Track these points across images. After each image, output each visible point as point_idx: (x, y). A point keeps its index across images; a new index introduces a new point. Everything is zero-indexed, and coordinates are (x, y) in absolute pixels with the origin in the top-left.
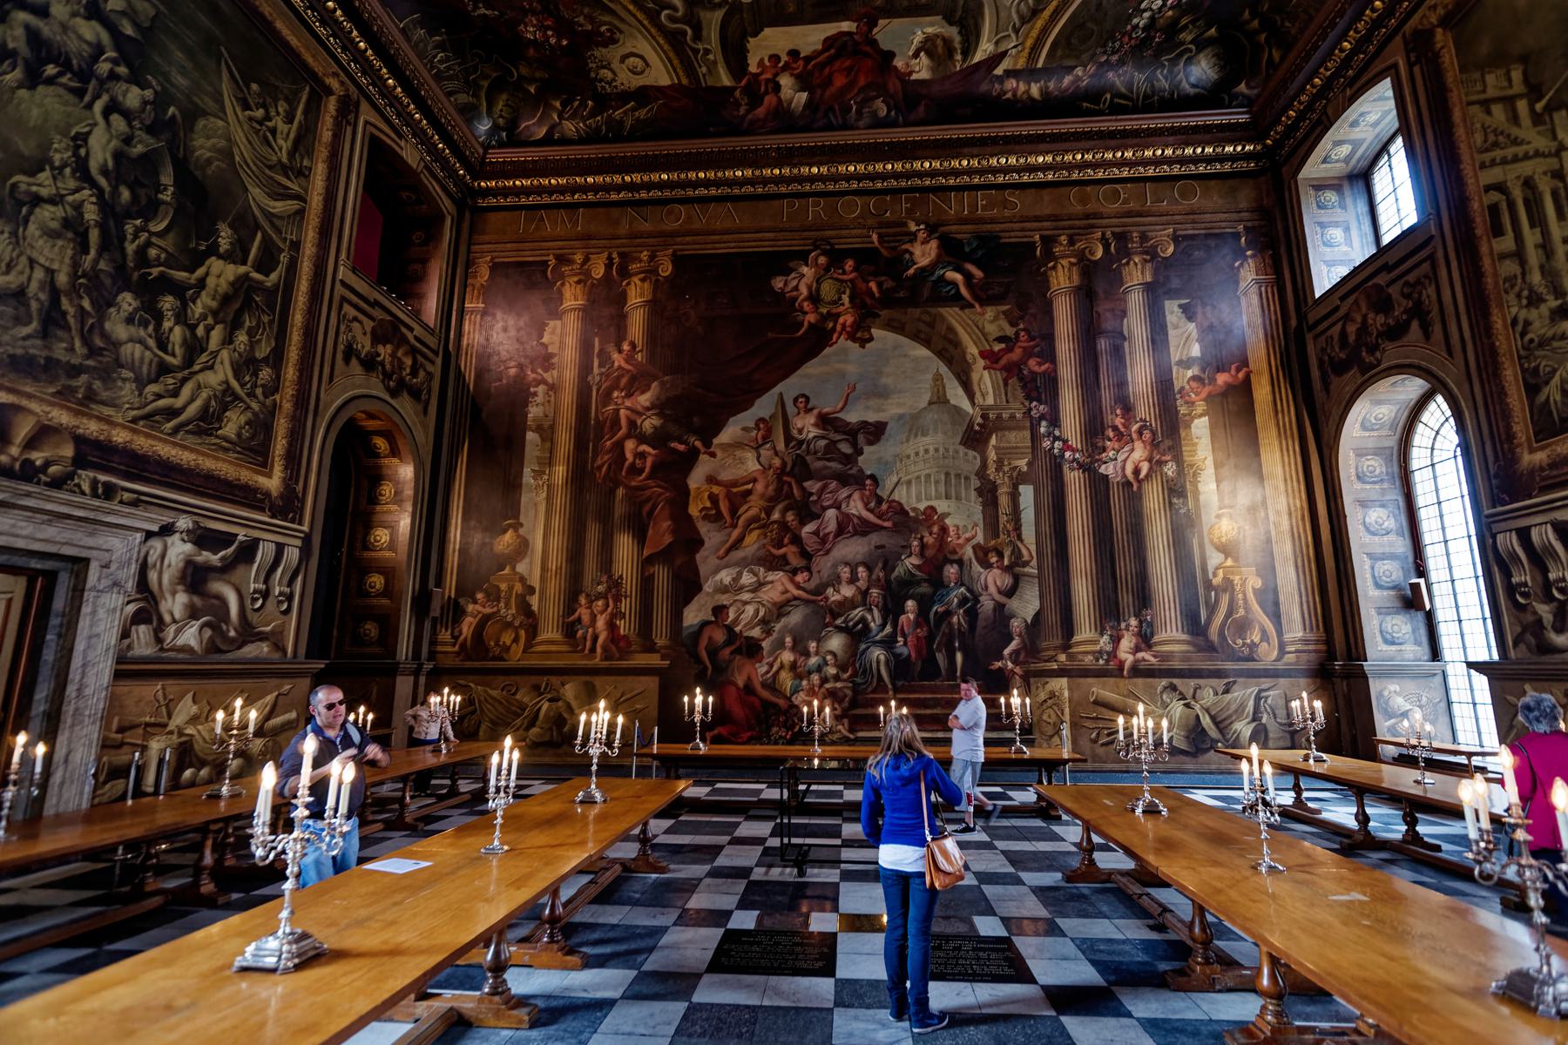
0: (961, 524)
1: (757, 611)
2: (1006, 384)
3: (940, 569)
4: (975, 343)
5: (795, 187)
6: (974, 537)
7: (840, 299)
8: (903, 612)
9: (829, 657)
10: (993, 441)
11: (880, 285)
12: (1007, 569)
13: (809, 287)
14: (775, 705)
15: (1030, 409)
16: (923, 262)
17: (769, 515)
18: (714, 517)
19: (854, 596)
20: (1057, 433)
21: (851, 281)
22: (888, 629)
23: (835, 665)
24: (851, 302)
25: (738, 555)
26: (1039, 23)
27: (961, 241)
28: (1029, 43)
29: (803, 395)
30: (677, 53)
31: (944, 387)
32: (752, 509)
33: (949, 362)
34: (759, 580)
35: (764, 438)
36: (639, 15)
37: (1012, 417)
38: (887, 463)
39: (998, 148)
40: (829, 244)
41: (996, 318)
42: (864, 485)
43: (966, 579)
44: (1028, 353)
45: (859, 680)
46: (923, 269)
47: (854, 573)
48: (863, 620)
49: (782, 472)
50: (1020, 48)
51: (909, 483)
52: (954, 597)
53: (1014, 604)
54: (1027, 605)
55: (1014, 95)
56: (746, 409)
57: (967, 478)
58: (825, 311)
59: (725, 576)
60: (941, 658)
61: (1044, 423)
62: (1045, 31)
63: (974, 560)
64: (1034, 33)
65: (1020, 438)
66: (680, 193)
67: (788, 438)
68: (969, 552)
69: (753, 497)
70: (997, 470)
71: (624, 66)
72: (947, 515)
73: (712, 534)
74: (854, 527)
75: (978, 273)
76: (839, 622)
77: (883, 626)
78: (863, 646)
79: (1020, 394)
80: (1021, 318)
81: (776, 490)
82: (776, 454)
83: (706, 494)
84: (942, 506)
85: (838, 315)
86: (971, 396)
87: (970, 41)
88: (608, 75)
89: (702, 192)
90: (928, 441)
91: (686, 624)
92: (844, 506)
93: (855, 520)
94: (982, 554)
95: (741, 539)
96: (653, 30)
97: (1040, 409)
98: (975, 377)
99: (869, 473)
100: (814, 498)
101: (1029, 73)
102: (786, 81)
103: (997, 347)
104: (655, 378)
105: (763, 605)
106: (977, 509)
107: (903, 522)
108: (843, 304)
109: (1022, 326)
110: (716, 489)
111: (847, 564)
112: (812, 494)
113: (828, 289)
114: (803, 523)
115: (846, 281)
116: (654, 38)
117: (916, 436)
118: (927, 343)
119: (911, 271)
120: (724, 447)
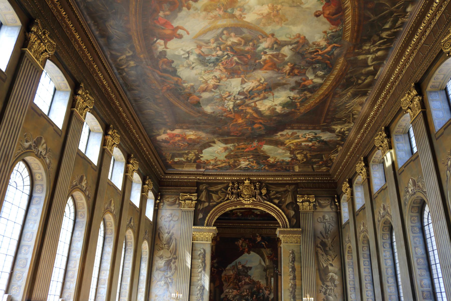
5: (239, 227)
8: (254, 297)
12: (269, 291)
16: (259, 241)
18: (226, 281)
24: (248, 246)
25: (229, 287)
48: (248, 298)
52: (262, 294)
53: (270, 296)
54: (272, 296)
59: (227, 290)
65: (272, 270)
67: (237, 269)
68: (264, 288)
69: (232, 278)
75: (267, 243)
84: (260, 281)
86: (265, 263)
89: (224, 226)
90: (258, 270)
94: (266, 288)
95: (230, 285)
97: (275, 266)
98: (266, 260)
102: (238, 213)
103: (269, 255)
106: (265, 282)
107: (254, 283)
110: (226, 277)
113: (244, 244)
114: (239, 282)
120: (228, 270)
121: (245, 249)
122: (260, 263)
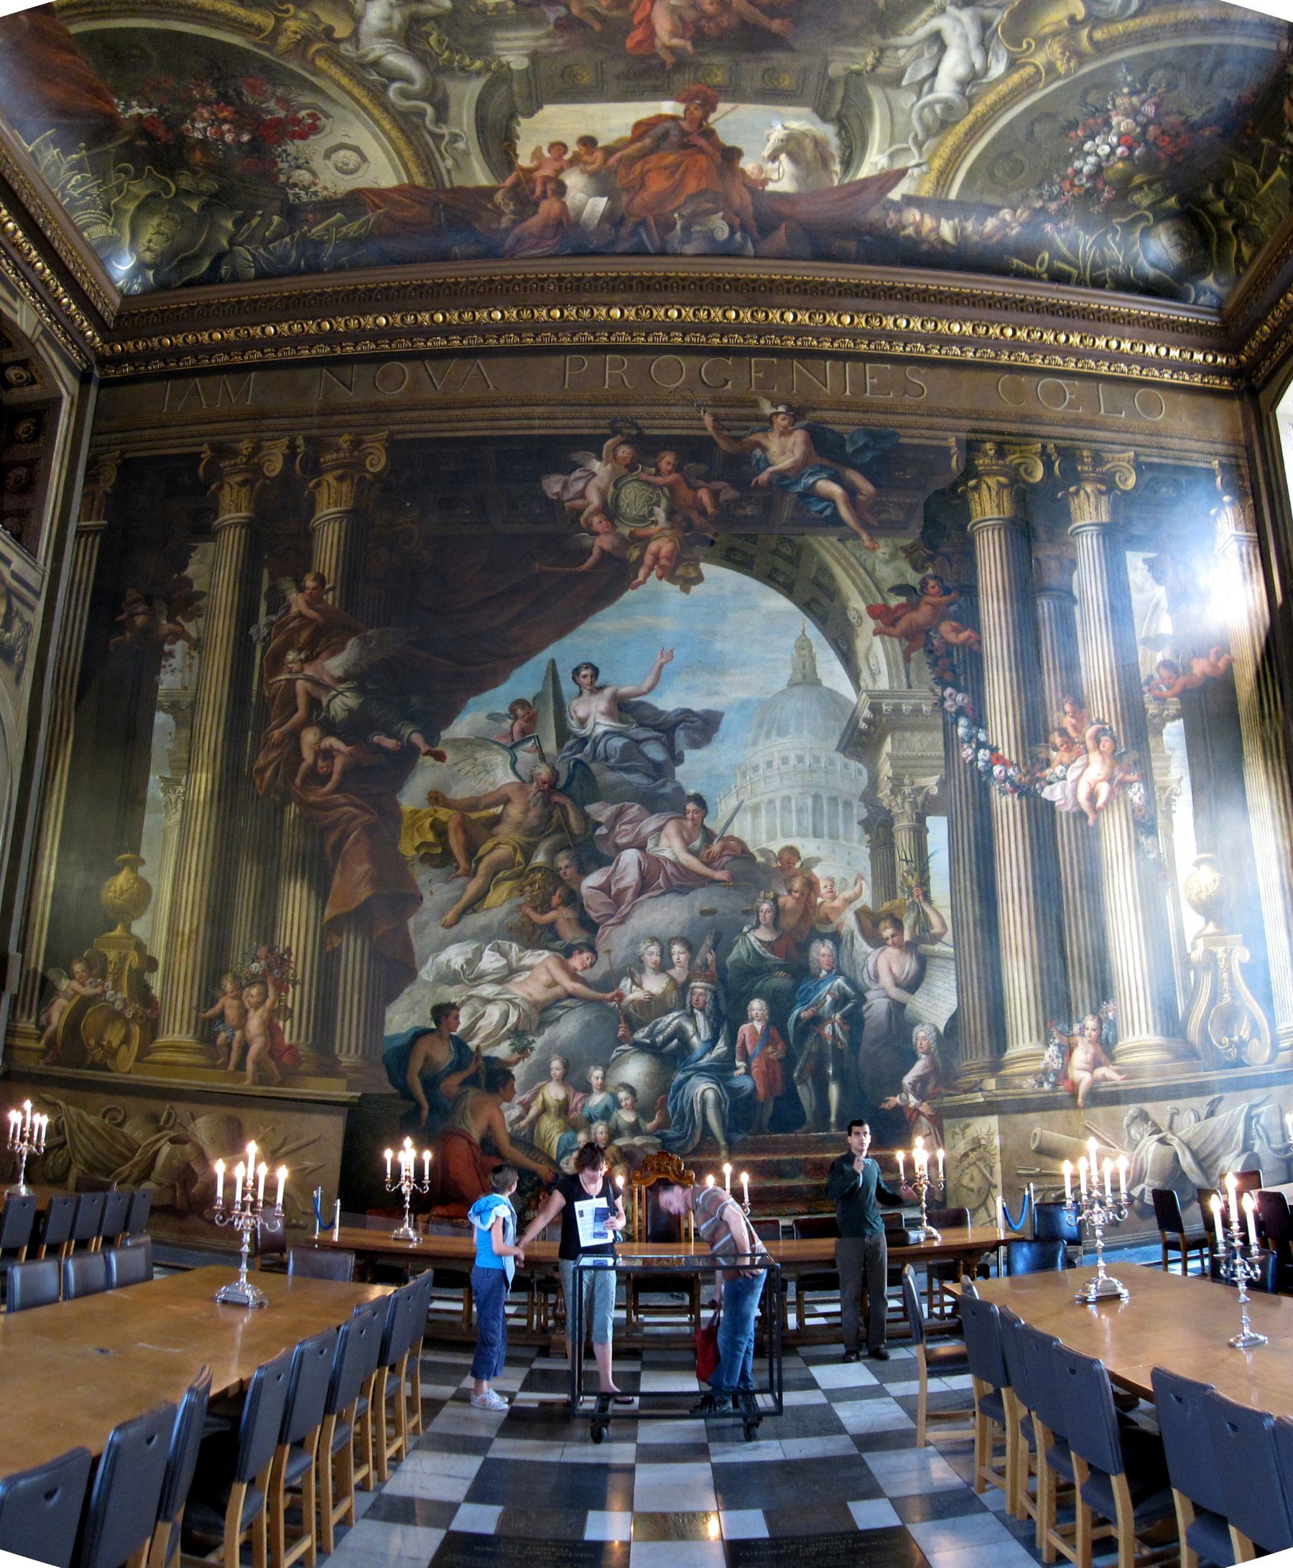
0: (837, 877)
1: (506, 1016)
2: (907, 660)
3: (804, 948)
4: (861, 593)
6: (857, 897)
7: (651, 513)
8: (745, 1018)
9: (622, 1095)
10: (887, 747)
11: (715, 495)
13: (603, 493)
14: (532, 1173)
15: (943, 700)
16: (783, 463)
17: (528, 855)
18: (440, 858)
19: (664, 993)
20: (982, 737)
21: (671, 487)
22: (721, 1047)
23: (633, 1108)
25: (476, 921)
26: (951, 140)
27: (839, 436)
28: (937, 163)
29: (589, 665)
30: (410, 142)
31: (813, 658)
32: (500, 848)
33: (822, 620)
34: (509, 964)
35: (523, 732)
36: (357, 91)
37: (917, 710)
38: (720, 777)
39: (894, 305)
40: (636, 426)
41: (893, 557)
42: (685, 812)
43: (846, 969)
44: (940, 615)
45: (671, 1133)
46: (782, 475)
47: (665, 955)
48: (679, 1033)
49: (551, 787)
50: (924, 168)
51: (756, 809)
55: (918, 231)
56: (496, 685)
57: (847, 805)
58: (626, 531)
59: (455, 956)
60: (805, 1094)
61: (963, 721)
62: (958, 153)
63: (857, 935)
64: (945, 152)
65: (928, 743)
66: (404, 345)
67: (563, 733)
68: (848, 921)
69: (504, 830)
70: (891, 791)
71: (330, 164)
72: (816, 861)
73: (434, 887)
74: (667, 879)
75: (865, 486)
76: (640, 1035)
77: (712, 1043)
78: (679, 1076)
79: (928, 675)
80: (931, 559)
81: (540, 817)
82: (543, 758)
83: (428, 822)
84: (807, 848)
85: (647, 540)
86: (854, 676)
87: (852, 151)
88: (303, 176)
91: (387, 1033)
92: (650, 845)
93: (669, 869)
94: (870, 924)
95: (482, 896)
96: (376, 112)
98: (861, 645)
99: (692, 791)
100: (602, 831)
101: (938, 206)
103: (895, 601)
104: (351, 631)
105: (516, 1005)
108: (655, 523)
109: (930, 571)
111: (654, 939)
112: (598, 825)
113: (632, 497)
114: (583, 872)
115: (661, 487)
116: (376, 122)
117: (768, 735)
118: (787, 589)
119: (763, 477)
120: (457, 743)
121: (645, 540)
122: (807, 678)
